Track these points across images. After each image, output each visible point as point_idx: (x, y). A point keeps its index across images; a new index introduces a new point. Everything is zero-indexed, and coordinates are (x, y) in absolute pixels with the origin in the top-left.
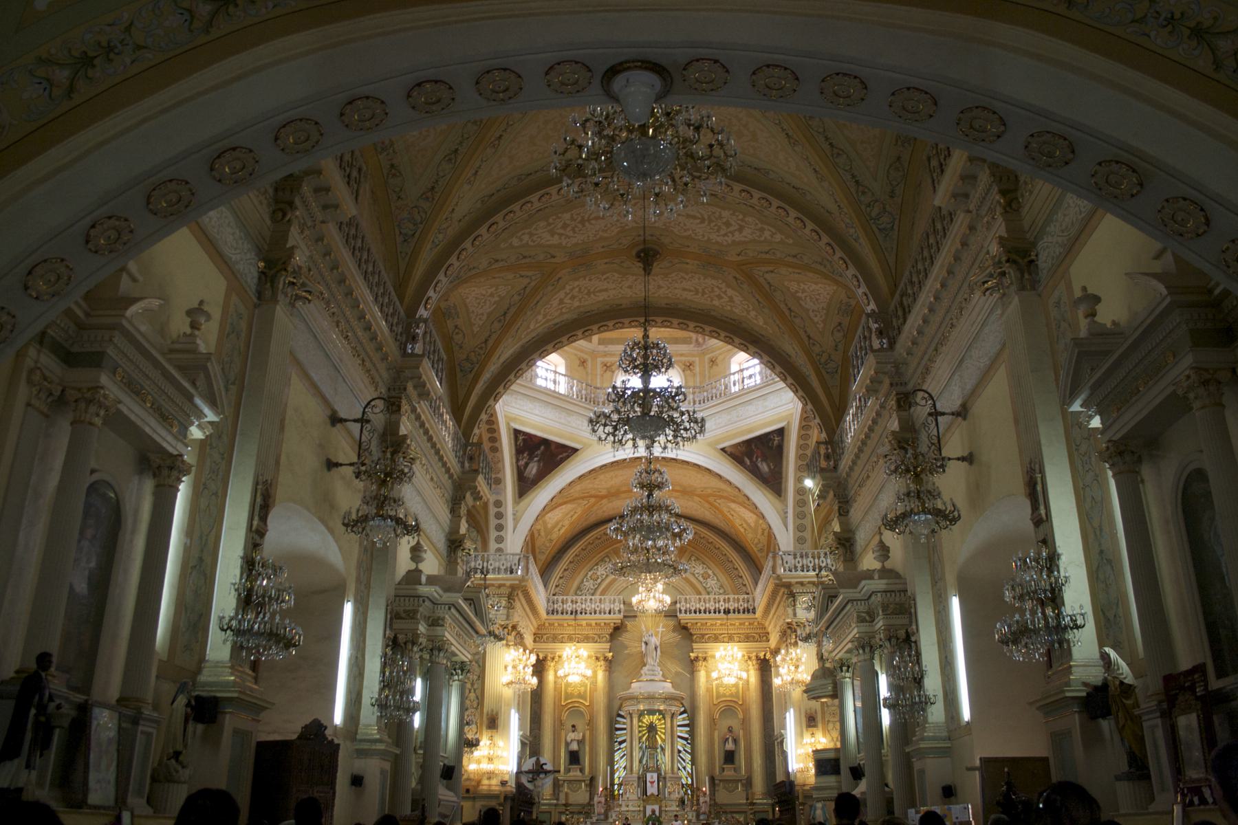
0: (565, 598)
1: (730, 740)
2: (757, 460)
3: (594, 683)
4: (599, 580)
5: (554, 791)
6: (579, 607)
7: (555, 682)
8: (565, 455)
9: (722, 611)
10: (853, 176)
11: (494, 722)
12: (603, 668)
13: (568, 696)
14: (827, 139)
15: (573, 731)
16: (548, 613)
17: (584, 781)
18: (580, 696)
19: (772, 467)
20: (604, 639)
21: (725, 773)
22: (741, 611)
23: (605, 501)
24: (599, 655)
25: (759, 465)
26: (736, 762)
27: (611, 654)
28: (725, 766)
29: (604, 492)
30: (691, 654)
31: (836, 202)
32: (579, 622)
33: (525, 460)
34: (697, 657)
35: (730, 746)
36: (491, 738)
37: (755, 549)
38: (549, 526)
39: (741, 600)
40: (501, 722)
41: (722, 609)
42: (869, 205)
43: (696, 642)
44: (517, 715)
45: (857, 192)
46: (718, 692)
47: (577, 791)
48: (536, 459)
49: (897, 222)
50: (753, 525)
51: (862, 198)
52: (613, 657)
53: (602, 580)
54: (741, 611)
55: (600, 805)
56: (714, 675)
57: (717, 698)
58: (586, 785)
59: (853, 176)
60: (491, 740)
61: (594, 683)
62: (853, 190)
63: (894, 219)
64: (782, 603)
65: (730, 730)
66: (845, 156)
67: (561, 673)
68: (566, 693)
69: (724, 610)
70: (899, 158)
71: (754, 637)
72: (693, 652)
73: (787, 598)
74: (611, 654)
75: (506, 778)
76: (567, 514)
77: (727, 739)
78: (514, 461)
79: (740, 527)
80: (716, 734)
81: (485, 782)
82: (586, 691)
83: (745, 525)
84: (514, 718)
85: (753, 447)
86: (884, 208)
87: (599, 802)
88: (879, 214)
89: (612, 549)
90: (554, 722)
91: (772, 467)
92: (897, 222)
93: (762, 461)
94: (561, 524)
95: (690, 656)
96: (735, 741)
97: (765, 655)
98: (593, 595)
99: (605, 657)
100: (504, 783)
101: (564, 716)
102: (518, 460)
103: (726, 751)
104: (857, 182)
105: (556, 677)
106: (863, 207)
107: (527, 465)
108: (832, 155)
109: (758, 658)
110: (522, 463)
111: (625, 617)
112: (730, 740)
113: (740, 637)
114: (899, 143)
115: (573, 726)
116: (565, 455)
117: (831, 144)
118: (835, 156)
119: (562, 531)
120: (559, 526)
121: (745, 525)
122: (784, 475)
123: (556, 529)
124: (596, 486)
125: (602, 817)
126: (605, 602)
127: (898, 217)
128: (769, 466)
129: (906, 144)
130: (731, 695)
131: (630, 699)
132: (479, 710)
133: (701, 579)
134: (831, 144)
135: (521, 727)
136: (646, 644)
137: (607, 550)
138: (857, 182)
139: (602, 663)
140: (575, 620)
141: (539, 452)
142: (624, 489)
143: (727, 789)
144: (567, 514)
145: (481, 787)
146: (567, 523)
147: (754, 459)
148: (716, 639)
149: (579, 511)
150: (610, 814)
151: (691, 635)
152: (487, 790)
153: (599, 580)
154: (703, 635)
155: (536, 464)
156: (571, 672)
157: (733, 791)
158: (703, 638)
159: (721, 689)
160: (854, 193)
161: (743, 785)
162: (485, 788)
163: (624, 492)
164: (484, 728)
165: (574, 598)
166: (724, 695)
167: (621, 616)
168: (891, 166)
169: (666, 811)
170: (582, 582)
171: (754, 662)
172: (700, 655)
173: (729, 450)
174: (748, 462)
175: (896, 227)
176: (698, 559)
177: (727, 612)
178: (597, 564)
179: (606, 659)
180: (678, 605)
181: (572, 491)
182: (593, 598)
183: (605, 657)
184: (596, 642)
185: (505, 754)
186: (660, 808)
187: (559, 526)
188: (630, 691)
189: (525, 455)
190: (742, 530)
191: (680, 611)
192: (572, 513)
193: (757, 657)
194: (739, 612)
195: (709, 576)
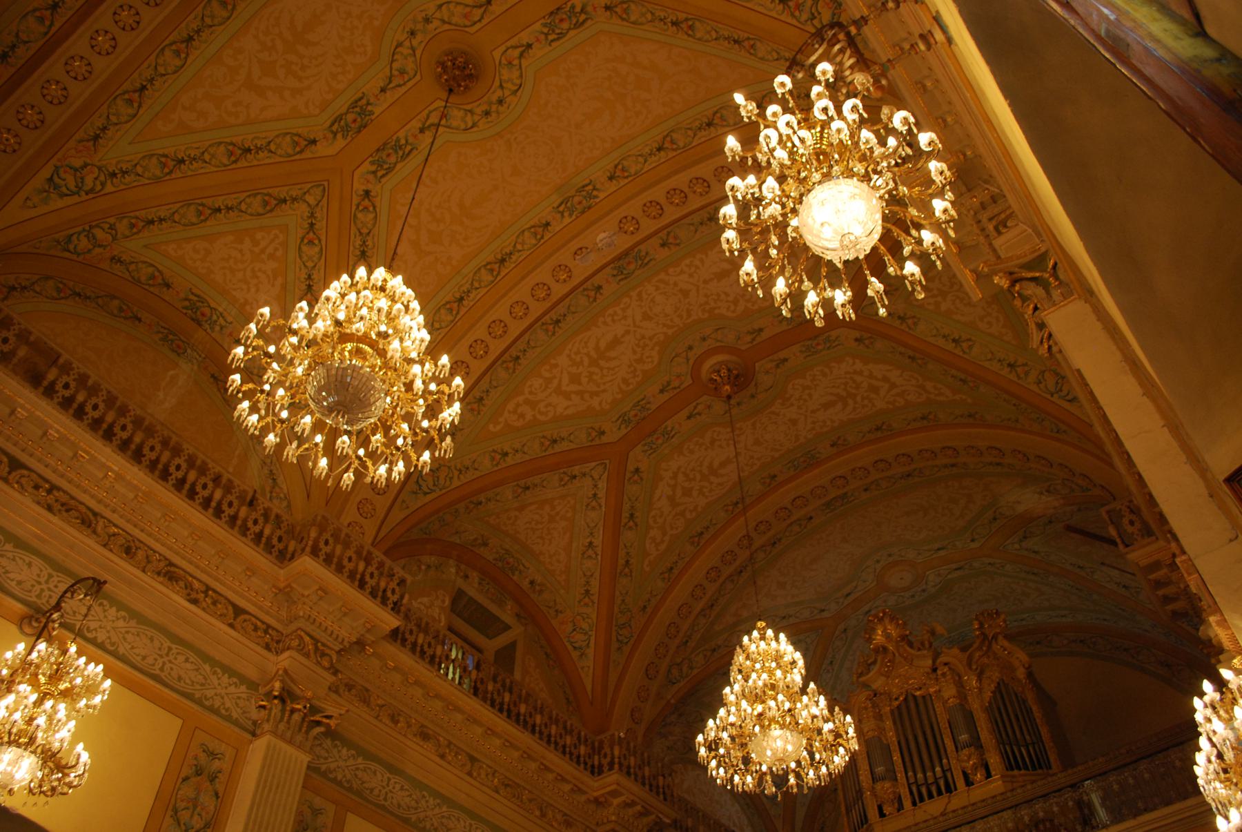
10: (161, 220)
14: (229, 209)
31: (125, 173)
42: (112, 227)
45: (137, 218)
49: (75, 257)
51: (125, 222)
59: (161, 220)
62: (142, 214)
63: (79, 255)
66: (194, 220)
70: (168, 286)
86: (100, 246)
88: (94, 238)
92: (75, 257)
104: (152, 222)
106: (112, 220)
108: (202, 205)
114: (192, 297)
117: (219, 210)
118: (200, 208)
127: (80, 259)
129: (187, 303)
134: (219, 210)
138: (152, 222)
160: (137, 213)
168: (159, 271)
175: (67, 255)
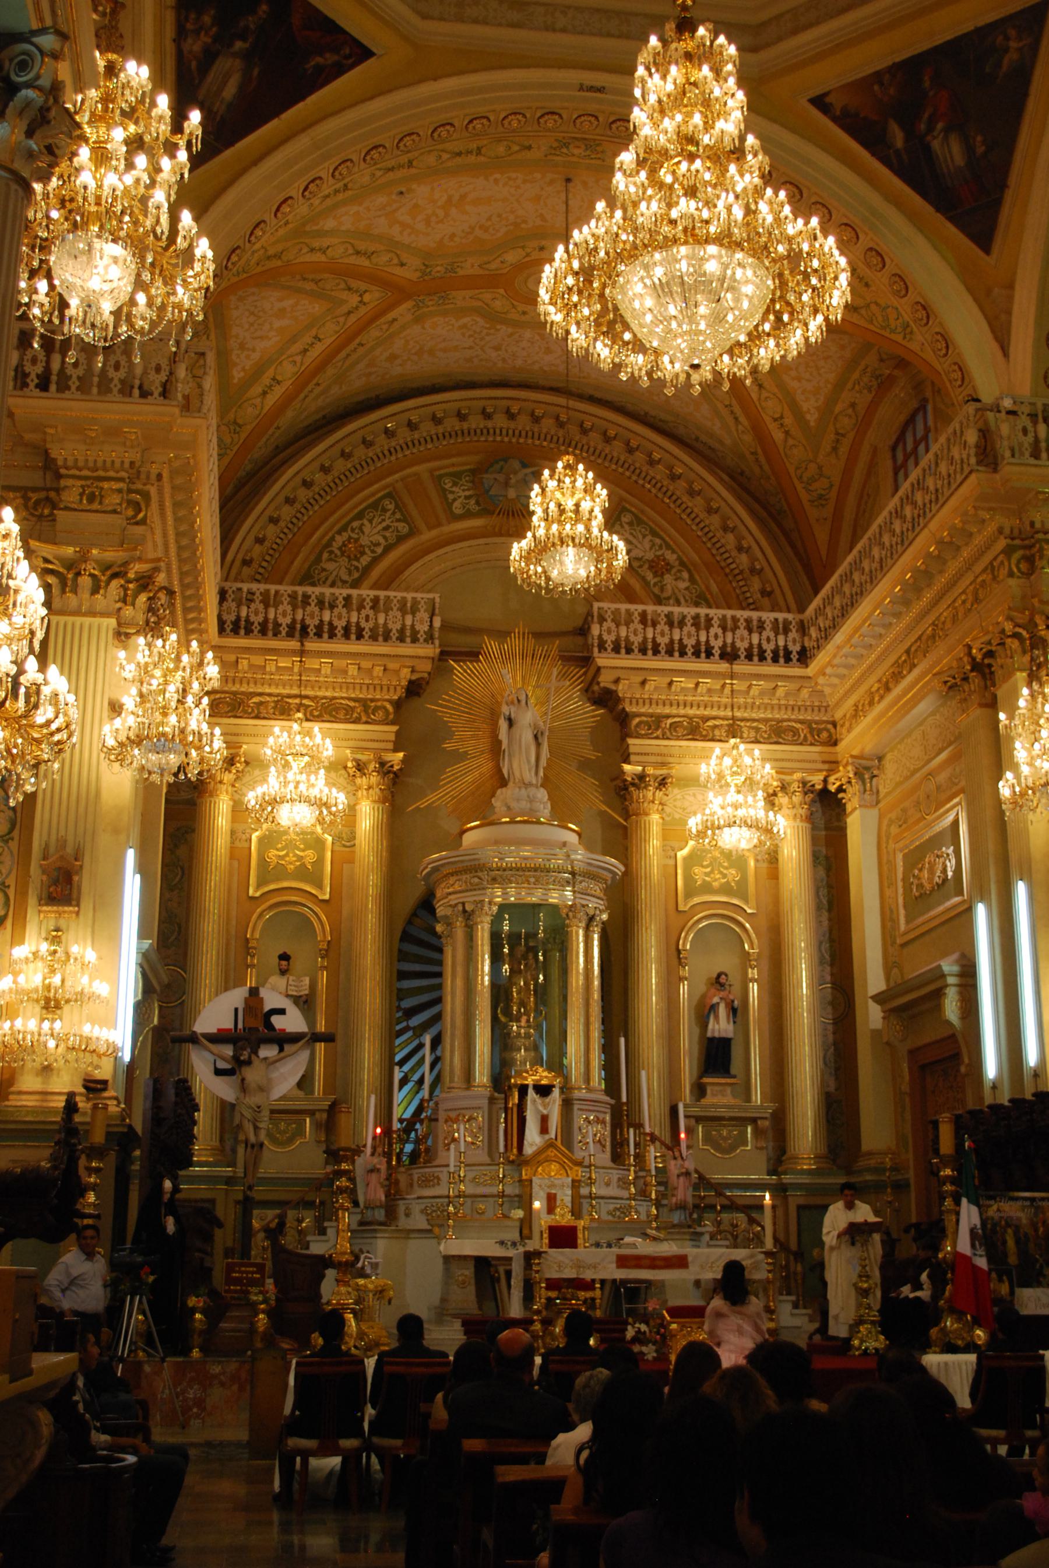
0: (273, 588)
1: (722, 1010)
2: (930, 129)
3: (347, 839)
4: (365, 560)
5: (222, 1140)
6: (312, 617)
7: (233, 832)
8: (331, 58)
9: (716, 652)
11: (69, 879)
12: (375, 793)
13: (267, 873)
15: (283, 972)
16: (221, 630)
17: (311, 1113)
18: (303, 873)
19: (980, 150)
20: (380, 715)
21: (709, 1099)
22: (769, 655)
23: (403, 311)
24: (363, 757)
25: (936, 145)
26: (736, 1067)
27: (401, 755)
28: (705, 1080)
29: (409, 274)
30: (627, 767)
32: (312, 663)
33: (205, 39)
34: (642, 777)
35: (721, 1026)
36: (55, 937)
37: (804, 496)
38: (237, 375)
39: (768, 626)
40: (86, 882)
41: (716, 644)
43: (639, 736)
44: (138, 877)
46: (689, 878)
47: (290, 1141)
48: (239, 45)
50: (812, 418)
52: (404, 761)
53: (375, 560)
54: (769, 655)
55: (374, 1177)
56: (694, 823)
57: (688, 895)
58: (317, 1126)
60: (55, 940)
61: (347, 839)
64: (969, 578)
65: (719, 982)
67: (252, 798)
68: (263, 862)
69: (723, 648)
71: (795, 732)
72: (627, 761)
73: (1008, 551)
74: (401, 755)
75: (104, 1071)
76: (293, 340)
77: (713, 1008)
78: (170, 32)
79: (772, 427)
80: (684, 989)
81: (29, 1082)
82: (320, 862)
83: (788, 420)
84: (132, 886)
85: (927, 84)
87: (373, 1170)
89: (402, 480)
90: (228, 944)
91: (980, 150)
93: (947, 131)
94: (270, 373)
95: (623, 773)
96: (737, 1012)
97: (825, 781)
98: (356, 584)
99: (382, 764)
100: (94, 1087)
101: (254, 933)
102: (181, 33)
103: (711, 1040)
105: (239, 809)
107: (209, 57)
109: (807, 788)
110: (194, 46)
111: (444, 655)
112: (722, 1010)
113: (757, 730)
115: (284, 957)
116: (331, 58)
119: (271, 400)
120: (266, 380)
121: (788, 420)
122: (1013, 180)
123: (257, 389)
124: (395, 231)
125: (380, 1215)
126: (387, 610)
128: (969, 149)
130: (726, 889)
131: (467, 870)
132: (14, 845)
133: (649, 576)
135: (142, 935)
136: (511, 722)
137: (389, 480)
139: (374, 779)
140: (302, 653)
141: (251, 22)
142: (470, 267)
143: (718, 1147)
144: (293, 340)
145: (14, 1101)
146: (288, 371)
147: (923, 127)
148: (695, 731)
149: (330, 333)
150: (401, 1207)
151: (623, 719)
152: (34, 1110)
153: (365, 560)
154: (659, 719)
155: (238, 63)
156: (289, 790)
157: (732, 1148)
158: (656, 726)
159: (699, 873)
161: (758, 1133)
162: (30, 1102)
163: (471, 283)
164: (32, 901)
165: (300, 590)
166: (707, 888)
167: (431, 650)
169: (591, 1196)
170: (318, 560)
171: (797, 798)
172: (650, 771)
173: (837, 101)
174: (898, 137)
176: (640, 522)
177: (729, 655)
178: (360, 516)
179: (384, 768)
180: (595, 630)
181: (330, 224)
182: (354, 592)
183: (382, 764)
184: (357, 721)
185: (102, 988)
186: (576, 1184)
187: (266, 380)
188: (460, 852)
189: (207, 19)
190: (778, 436)
191: (602, 646)
192: (307, 339)
193: (804, 783)
194: (762, 658)
195: (668, 567)
